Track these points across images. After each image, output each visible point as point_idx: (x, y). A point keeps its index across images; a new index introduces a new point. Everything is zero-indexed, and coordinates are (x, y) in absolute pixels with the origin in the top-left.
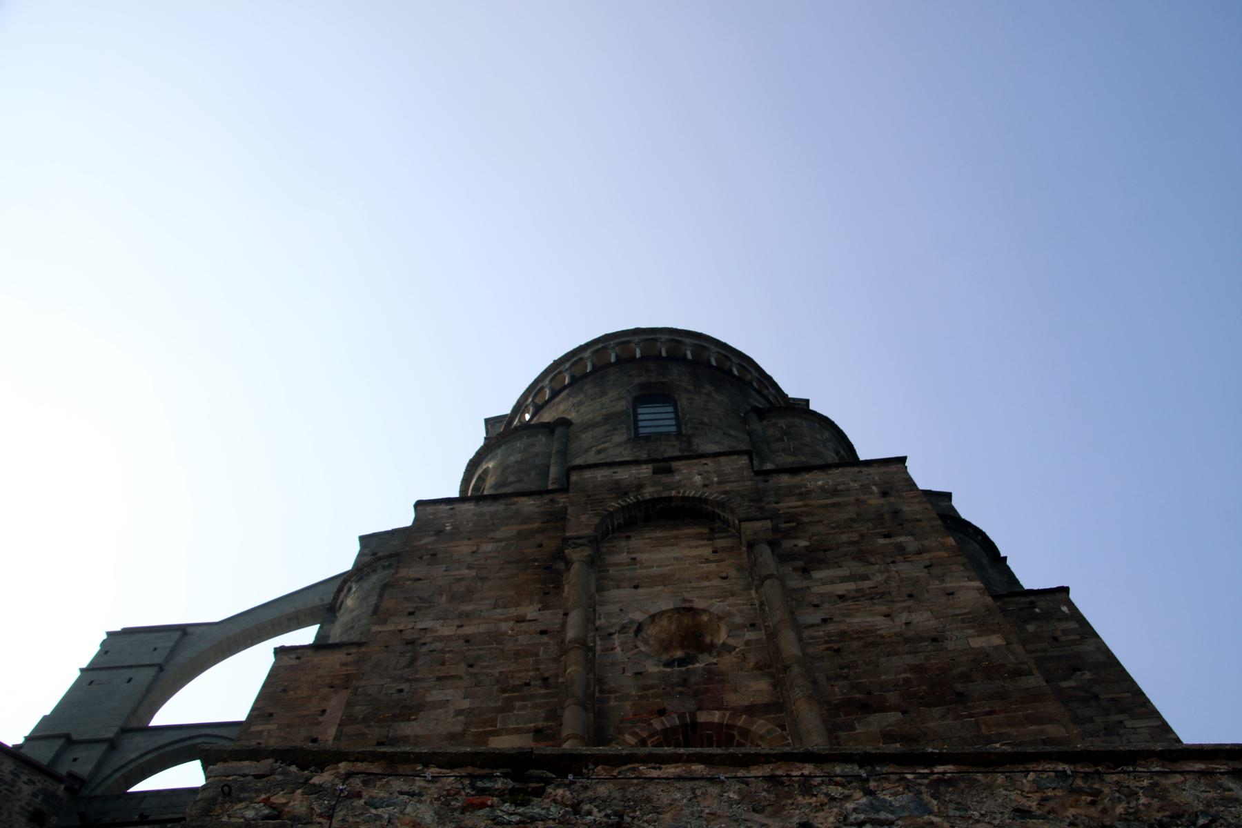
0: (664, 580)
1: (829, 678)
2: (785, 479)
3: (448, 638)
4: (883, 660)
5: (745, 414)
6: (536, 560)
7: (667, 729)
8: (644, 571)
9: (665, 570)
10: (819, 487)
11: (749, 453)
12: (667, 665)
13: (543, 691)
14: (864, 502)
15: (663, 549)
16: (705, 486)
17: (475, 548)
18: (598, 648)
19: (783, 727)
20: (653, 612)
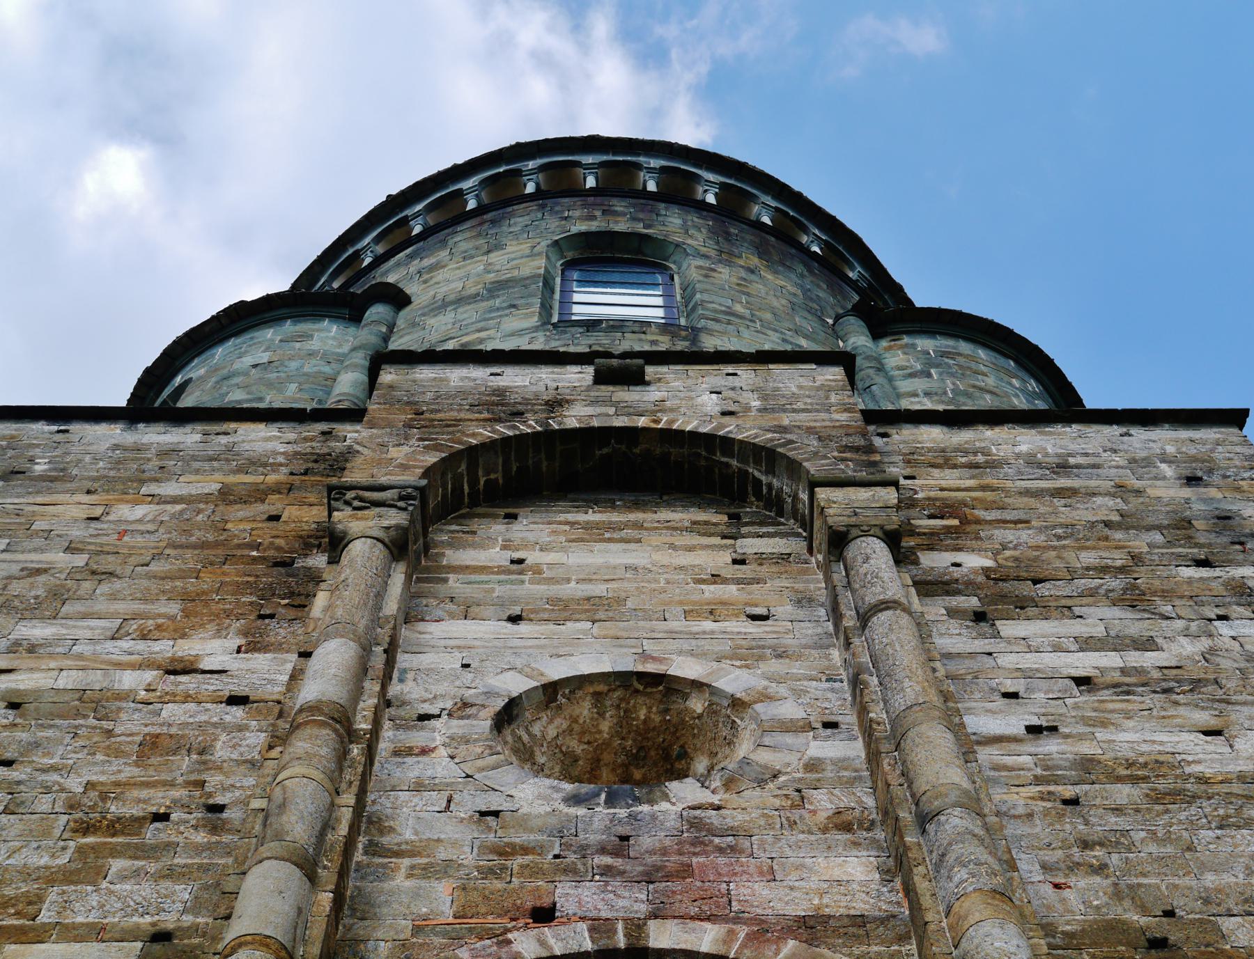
1: (1045, 867)
2: (932, 435)
4: (1209, 834)
5: (837, 318)
6: (257, 547)
8: (542, 589)
9: (599, 589)
10: (1018, 456)
11: (847, 361)
12: (575, 800)
13: (201, 837)
14: (1138, 492)
15: (599, 546)
16: (724, 414)
17: (98, 511)
18: (384, 747)
20: (557, 671)
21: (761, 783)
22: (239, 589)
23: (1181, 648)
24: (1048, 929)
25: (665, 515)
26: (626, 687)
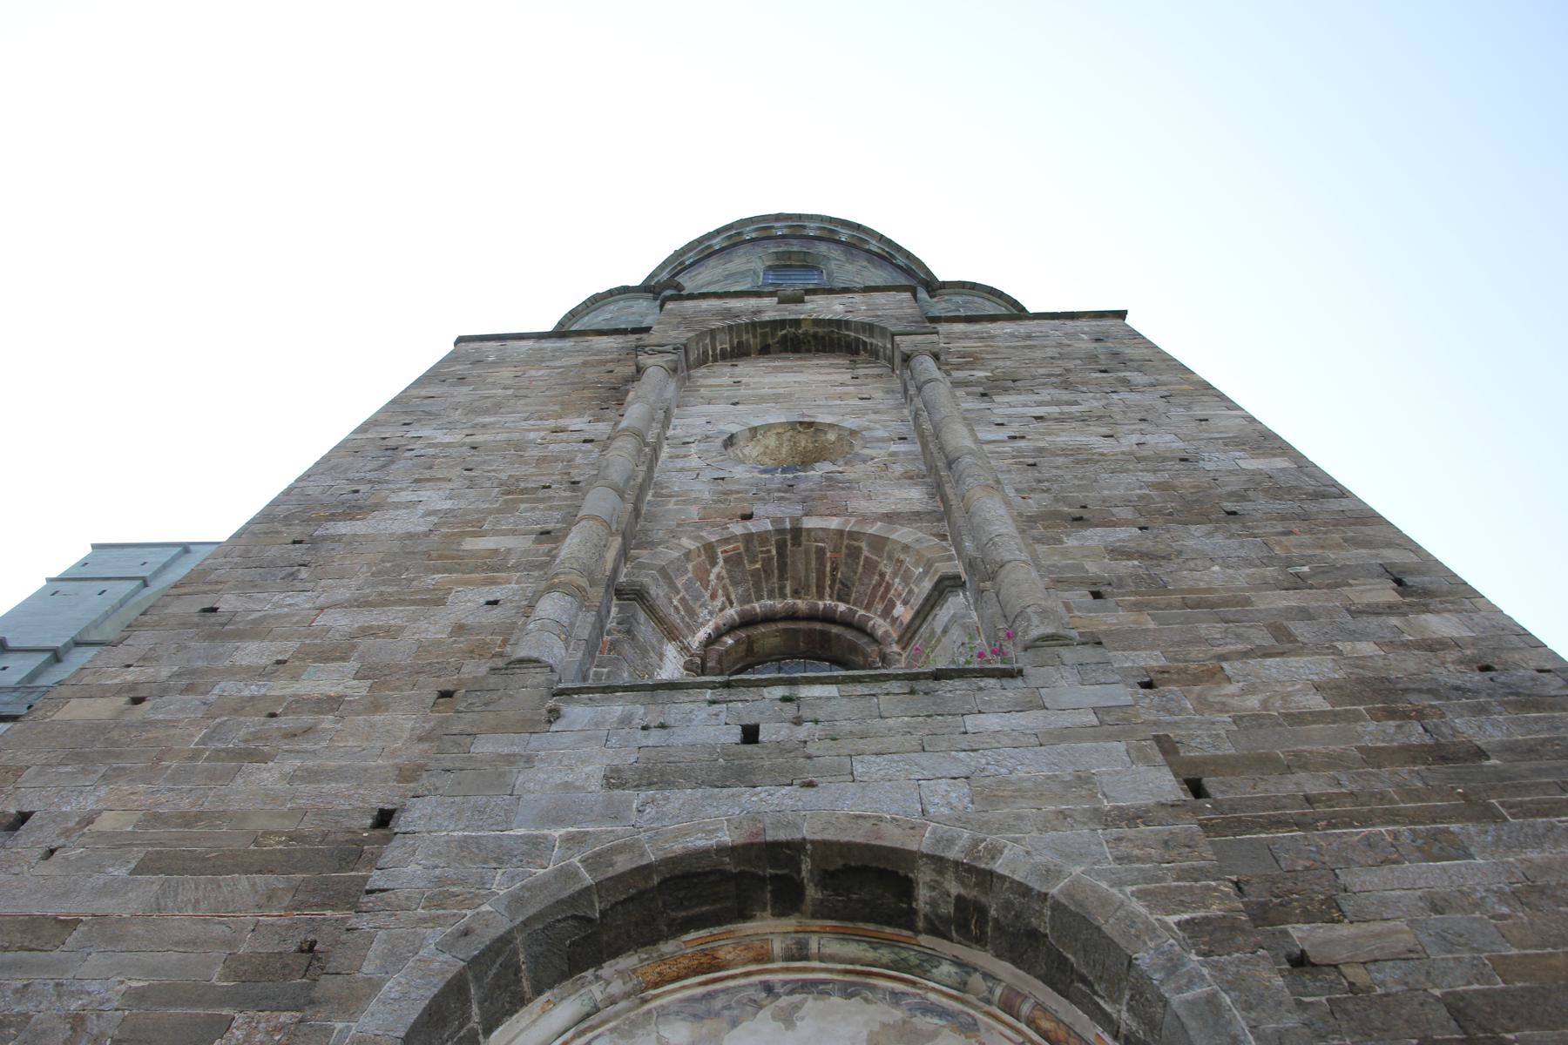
0: (776, 398)
2: (960, 327)
3: (449, 445)
7: (752, 534)
13: (568, 494)
19: (943, 537)
20: (756, 423)
21: (864, 461)
22: (591, 399)
23: (1091, 403)
24: (1020, 515)
25: (815, 362)
26: (793, 429)
